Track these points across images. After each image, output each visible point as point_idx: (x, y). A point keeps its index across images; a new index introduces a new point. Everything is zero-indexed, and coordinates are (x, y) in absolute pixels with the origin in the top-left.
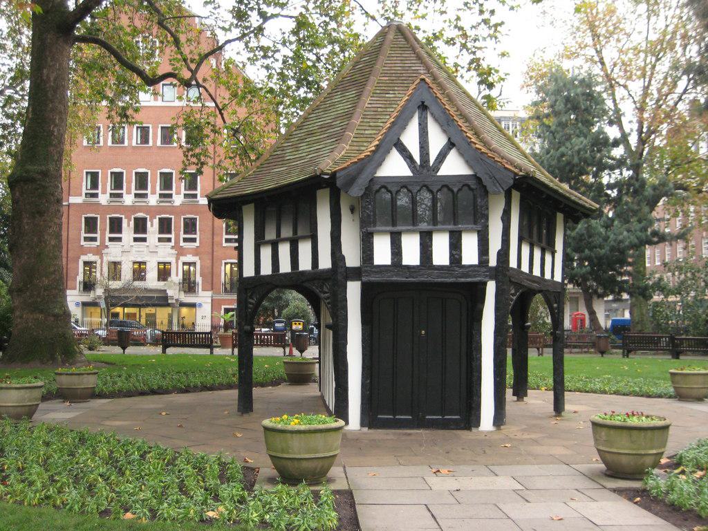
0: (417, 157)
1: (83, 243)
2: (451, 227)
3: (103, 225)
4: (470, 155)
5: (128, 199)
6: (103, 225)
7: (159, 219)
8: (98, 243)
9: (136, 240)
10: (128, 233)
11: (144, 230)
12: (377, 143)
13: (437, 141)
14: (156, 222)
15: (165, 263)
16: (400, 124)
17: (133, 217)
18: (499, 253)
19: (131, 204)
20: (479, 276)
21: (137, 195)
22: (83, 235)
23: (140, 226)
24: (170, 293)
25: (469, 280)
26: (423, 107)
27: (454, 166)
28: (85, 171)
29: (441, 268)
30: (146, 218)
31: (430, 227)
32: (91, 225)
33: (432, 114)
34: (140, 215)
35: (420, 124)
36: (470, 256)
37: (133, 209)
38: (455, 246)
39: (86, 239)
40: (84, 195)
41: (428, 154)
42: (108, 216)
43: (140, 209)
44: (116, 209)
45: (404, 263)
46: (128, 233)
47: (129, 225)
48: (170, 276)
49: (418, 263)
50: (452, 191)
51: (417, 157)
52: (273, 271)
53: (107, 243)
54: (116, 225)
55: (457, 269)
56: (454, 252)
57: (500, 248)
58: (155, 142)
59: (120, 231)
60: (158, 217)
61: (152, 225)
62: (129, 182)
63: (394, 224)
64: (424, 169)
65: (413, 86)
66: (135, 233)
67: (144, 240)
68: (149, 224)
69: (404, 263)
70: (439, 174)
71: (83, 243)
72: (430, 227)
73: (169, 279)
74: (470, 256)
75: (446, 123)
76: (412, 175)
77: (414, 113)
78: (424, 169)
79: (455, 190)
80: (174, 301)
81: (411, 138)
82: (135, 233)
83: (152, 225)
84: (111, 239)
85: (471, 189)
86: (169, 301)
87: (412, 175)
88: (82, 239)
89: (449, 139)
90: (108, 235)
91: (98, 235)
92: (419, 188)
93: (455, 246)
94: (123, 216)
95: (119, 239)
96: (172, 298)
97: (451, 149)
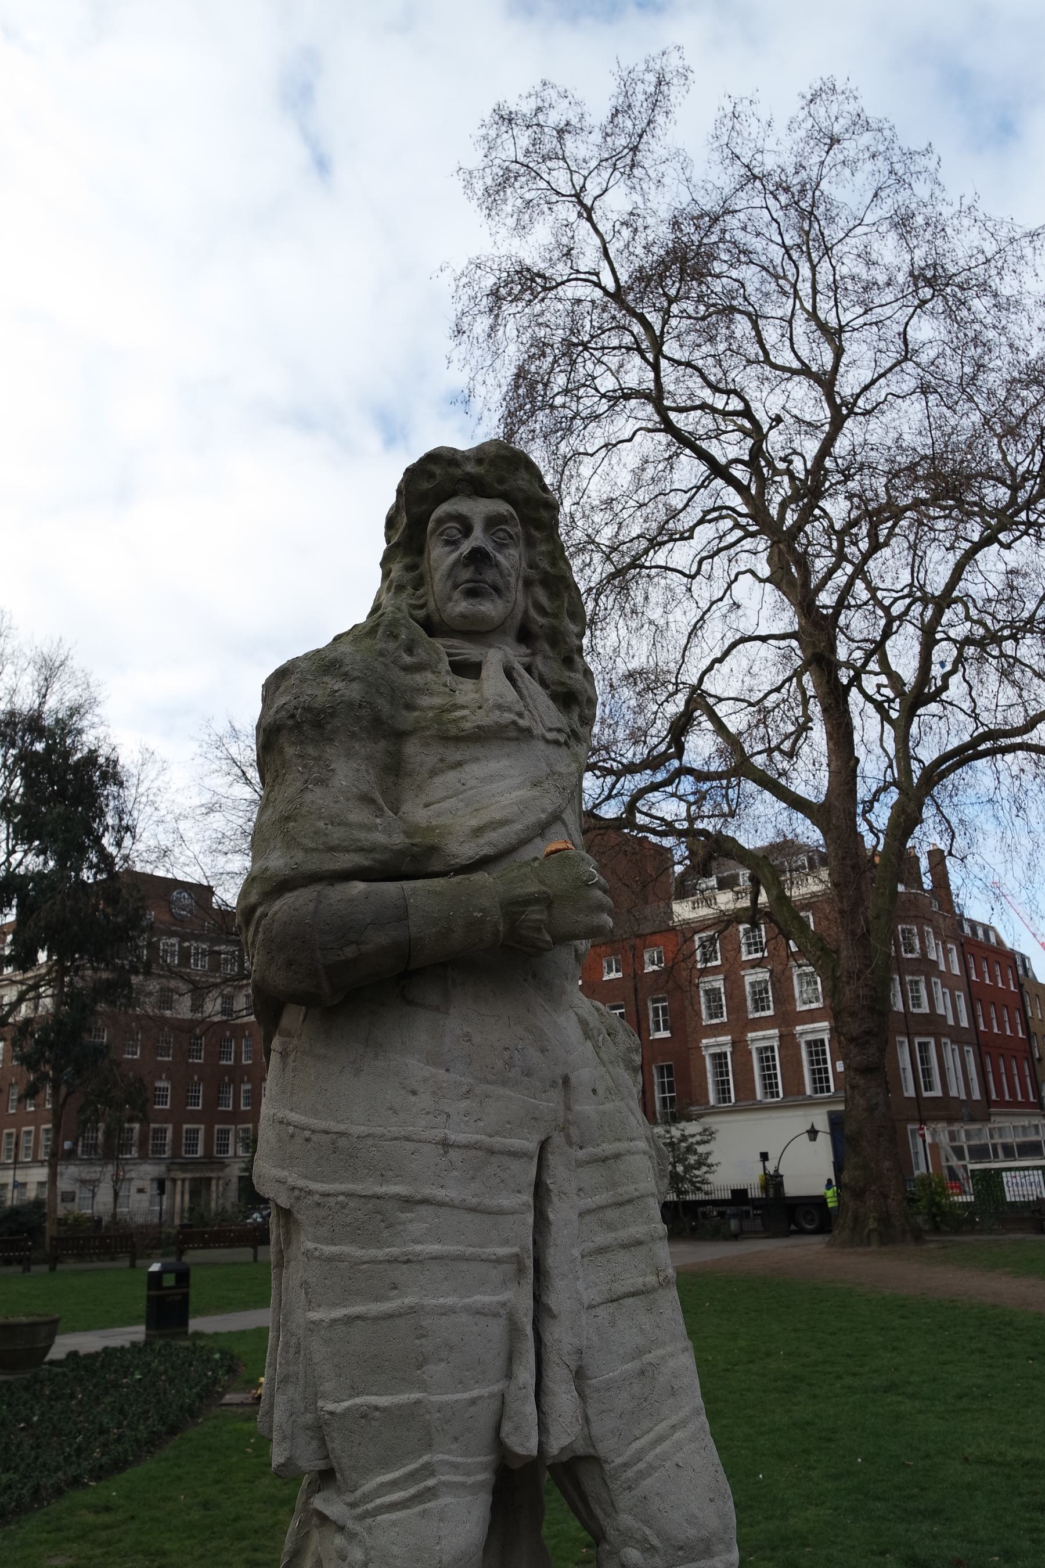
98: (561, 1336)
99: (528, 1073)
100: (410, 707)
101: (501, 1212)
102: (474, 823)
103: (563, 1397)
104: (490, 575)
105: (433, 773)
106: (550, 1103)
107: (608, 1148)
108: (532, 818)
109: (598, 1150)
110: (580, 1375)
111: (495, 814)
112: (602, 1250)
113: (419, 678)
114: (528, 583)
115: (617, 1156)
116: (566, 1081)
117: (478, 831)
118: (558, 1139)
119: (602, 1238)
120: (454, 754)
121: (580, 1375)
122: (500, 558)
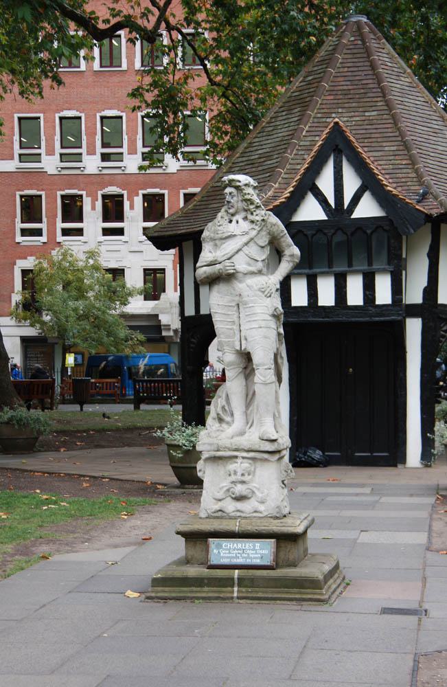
0: (332, 201)
1: (19, 239)
2: (365, 267)
3: (51, 207)
4: (383, 197)
5: (92, 164)
6: (51, 207)
7: (144, 195)
8: (44, 239)
9: (107, 232)
10: (93, 220)
11: (120, 217)
12: (292, 189)
13: (351, 183)
14: (138, 201)
15: (155, 271)
16: (315, 168)
17: (100, 193)
18: (425, 291)
19: (96, 172)
20: (393, 315)
21: (105, 157)
22: (19, 225)
23: (113, 209)
24: (164, 319)
25: (382, 319)
26: (338, 152)
27: (367, 209)
28: (16, 116)
29: (356, 307)
30: (122, 196)
31: (347, 269)
32: (31, 208)
33: (346, 156)
34: (113, 190)
35: (335, 167)
36: (384, 294)
37: (99, 180)
38: (369, 288)
39: (24, 232)
40: (16, 157)
41: (342, 198)
42: (59, 193)
43: (111, 180)
44: (71, 181)
45: (320, 304)
46: (93, 220)
47: (93, 208)
48: (164, 291)
49: (333, 304)
50: (365, 232)
51: (332, 201)
52: (196, 313)
53: (60, 238)
54: (72, 209)
55: (371, 308)
56: (368, 293)
57: (426, 284)
58: (131, 62)
59: (80, 219)
60: (141, 192)
61: (132, 207)
62: (92, 135)
63: (311, 267)
64: (339, 212)
65: (327, 130)
66: (105, 219)
67: (120, 232)
68: (127, 204)
69: (320, 304)
70: (353, 217)
71: (19, 239)
72: (347, 269)
73: (163, 296)
74: (384, 294)
75: (362, 168)
76: (326, 218)
77: (330, 156)
78: (339, 212)
79: (369, 232)
80: (171, 333)
81: (326, 182)
82: (105, 219)
83: (132, 207)
84: (66, 232)
85: (385, 230)
86: (164, 334)
87: (326, 218)
88: (18, 233)
89: (363, 182)
90: (60, 225)
91: (43, 226)
92: (333, 231)
93: (369, 288)
94: (84, 193)
95: (79, 232)
96: (168, 327)
97: (366, 191)
98: (243, 334)
99: (231, 294)
100: (217, 234)
101: (229, 315)
102: (222, 254)
103: (243, 342)
104: (231, 204)
105: (221, 245)
106: (237, 298)
107: (250, 305)
108: (233, 252)
109: (248, 306)
110: (246, 339)
111: (227, 252)
112: (249, 321)
113: (219, 228)
114: (242, 201)
115: (253, 306)
116: (240, 295)
117: (224, 255)
118: (240, 304)
119: (250, 319)
120: (224, 241)
121: (246, 339)
122: (232, 201)
